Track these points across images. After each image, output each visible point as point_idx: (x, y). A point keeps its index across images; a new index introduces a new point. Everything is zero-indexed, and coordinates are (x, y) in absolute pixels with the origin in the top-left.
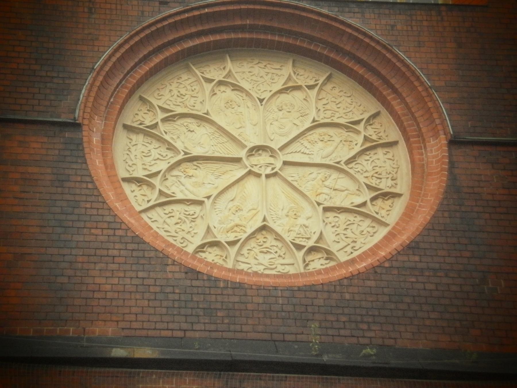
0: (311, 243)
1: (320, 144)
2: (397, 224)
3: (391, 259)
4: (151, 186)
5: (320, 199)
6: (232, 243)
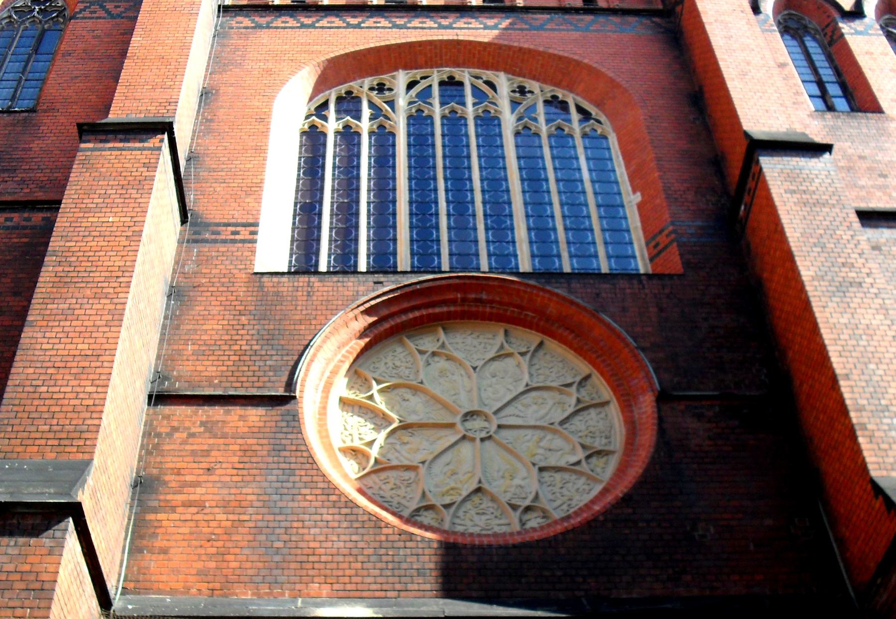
0: (527, 503)
1: (534, 407)
2: (611, 479)
3: (605, 512)
5: (536, 459)
6: (447, 506)
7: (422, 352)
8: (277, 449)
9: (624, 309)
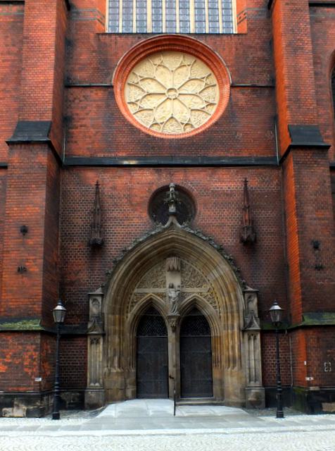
0: (186, 122)
1: (191, 87)
3: (209, 128)
4: (136, 104)
6: (162, 123)
7: (155, 65)
8: (108, 106)
9: (224, 49)
